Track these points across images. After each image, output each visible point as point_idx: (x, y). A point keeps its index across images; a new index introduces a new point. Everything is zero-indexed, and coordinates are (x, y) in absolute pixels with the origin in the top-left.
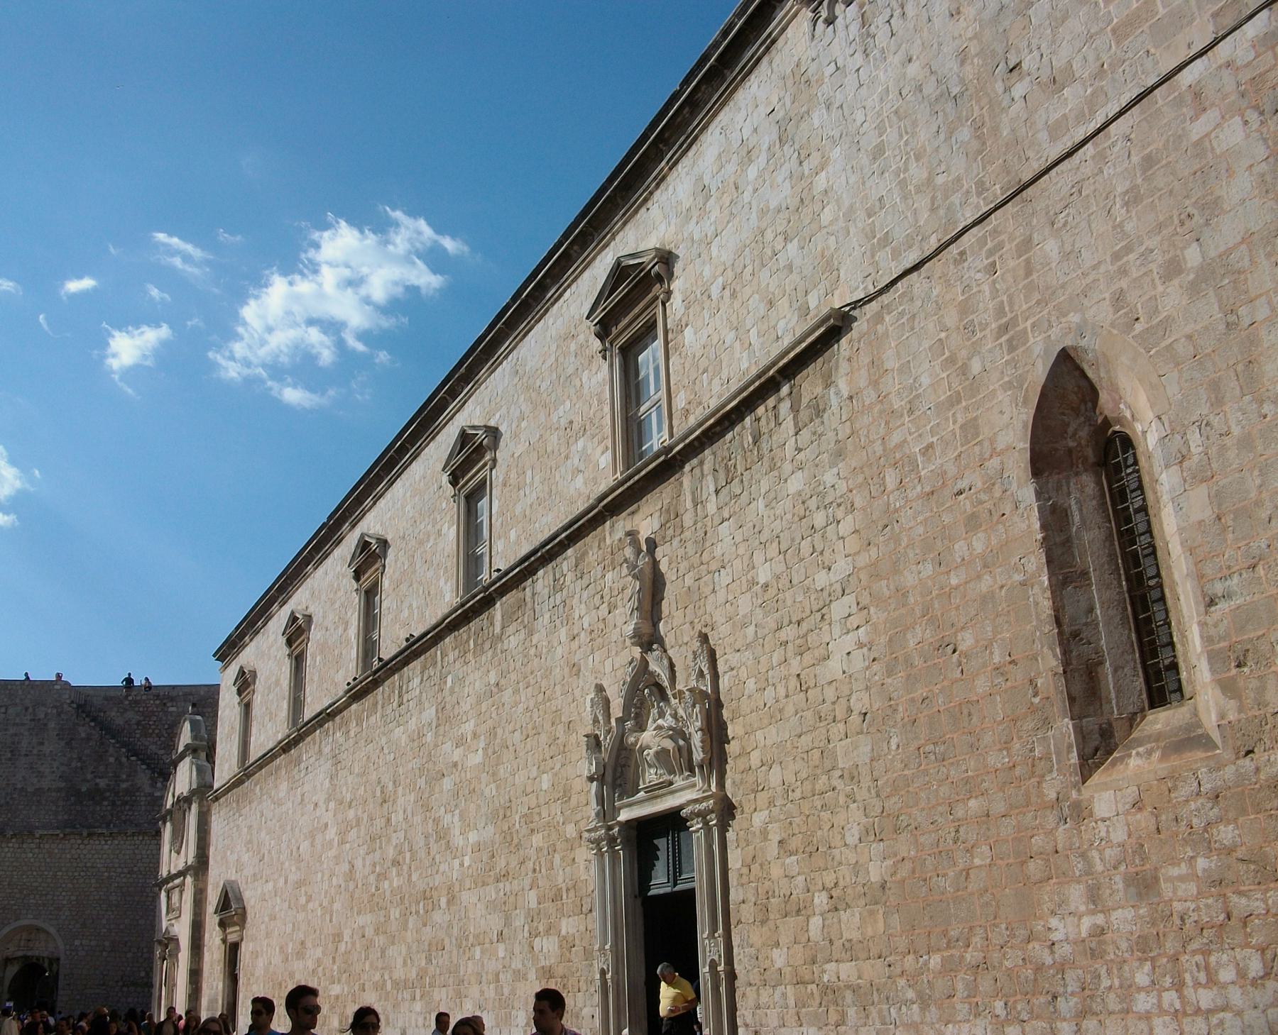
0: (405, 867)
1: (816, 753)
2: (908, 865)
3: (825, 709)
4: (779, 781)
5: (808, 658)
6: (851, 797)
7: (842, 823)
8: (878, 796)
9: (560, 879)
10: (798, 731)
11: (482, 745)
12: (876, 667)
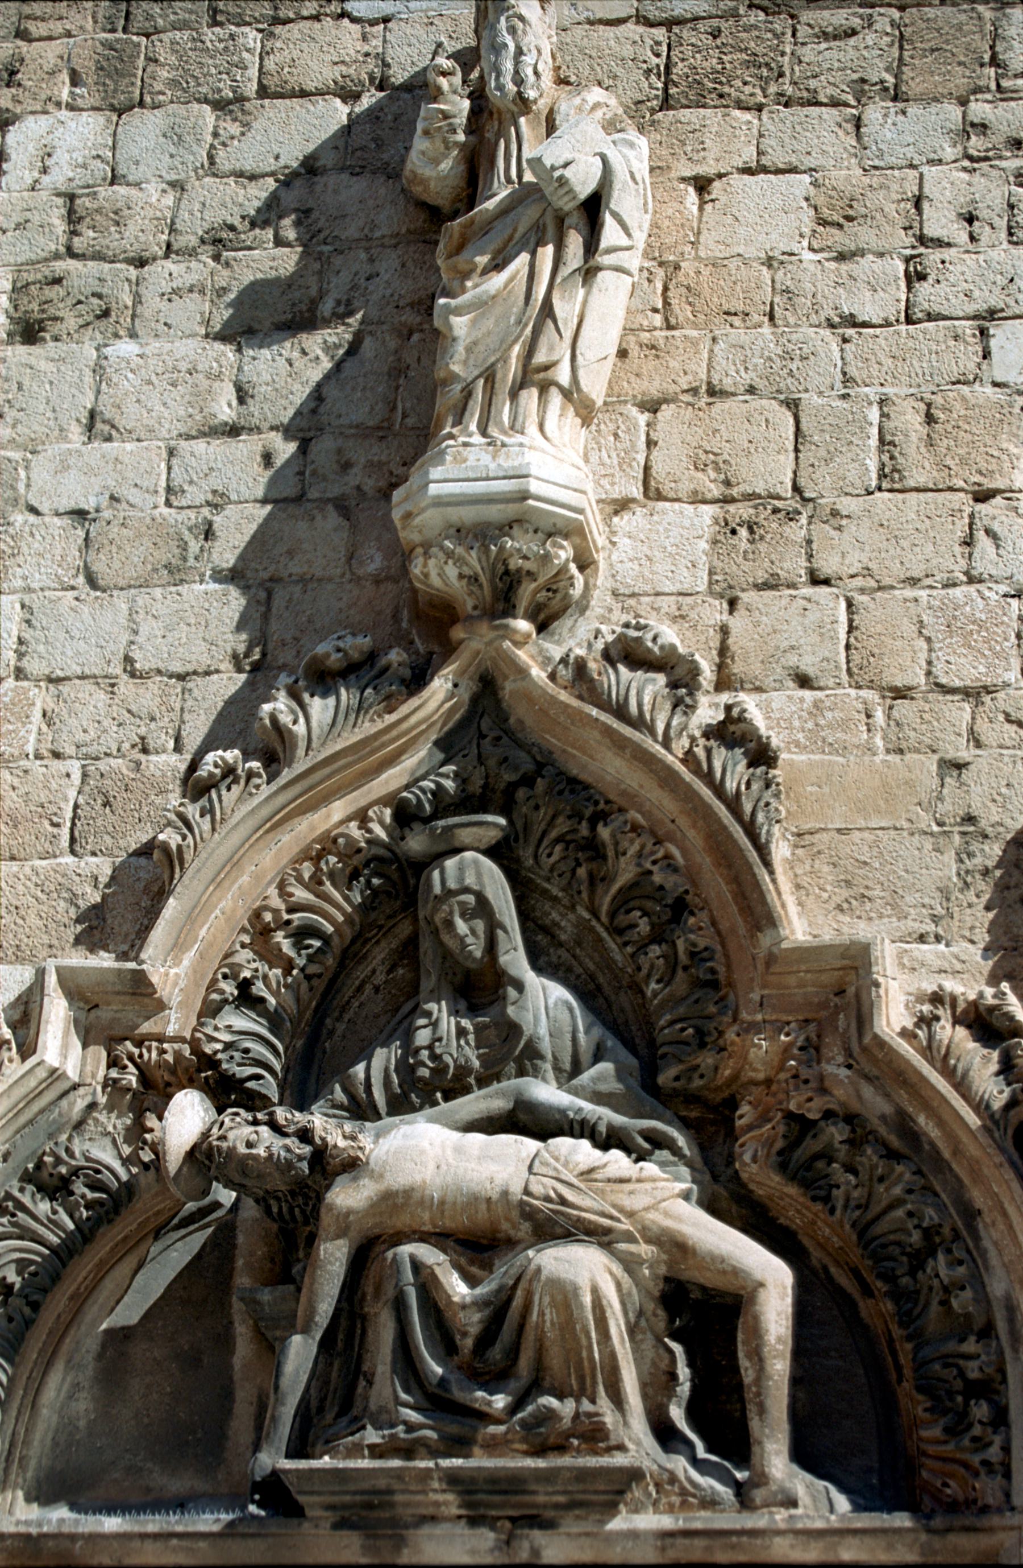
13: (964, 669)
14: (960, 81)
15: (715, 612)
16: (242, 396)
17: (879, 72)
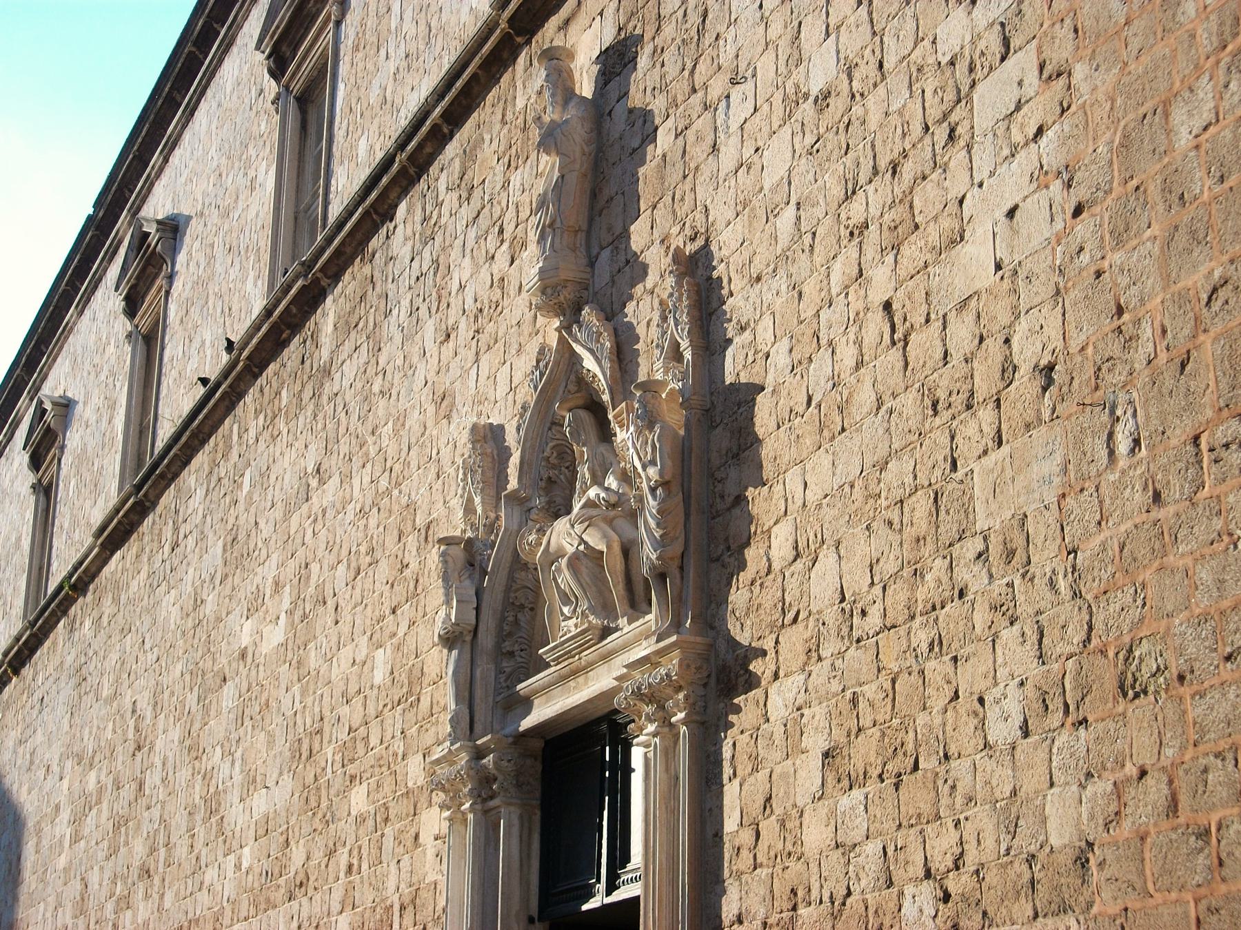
0: (157, 880)
1: (921, 504)
2: (1155, 788)
3: (944, 381)
4: (831, 593)
5: (912, 252)
6: (1005, 610)
7: (981, 685)
8: (1076, 594)
9: (391, 884)
10: (882, 451)
11: (286, 605)
12: (1083, 228)
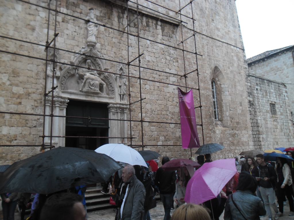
10: (158, 99)
13: (112, 56)
14: (111, 24)
15: (101, 50)
16: (76, 30)
17: (107, 22)
